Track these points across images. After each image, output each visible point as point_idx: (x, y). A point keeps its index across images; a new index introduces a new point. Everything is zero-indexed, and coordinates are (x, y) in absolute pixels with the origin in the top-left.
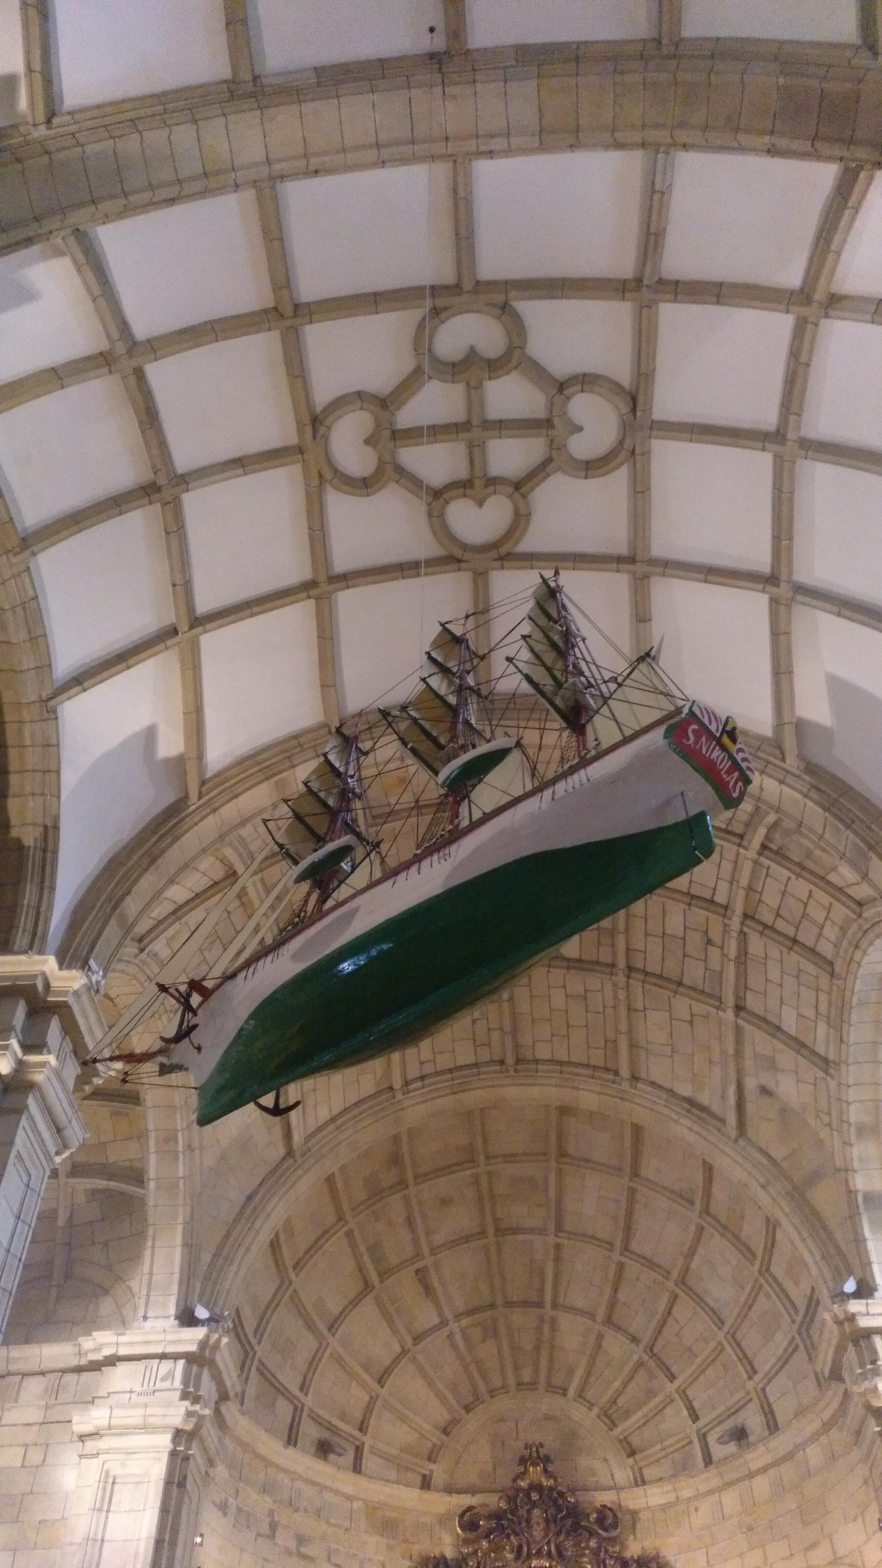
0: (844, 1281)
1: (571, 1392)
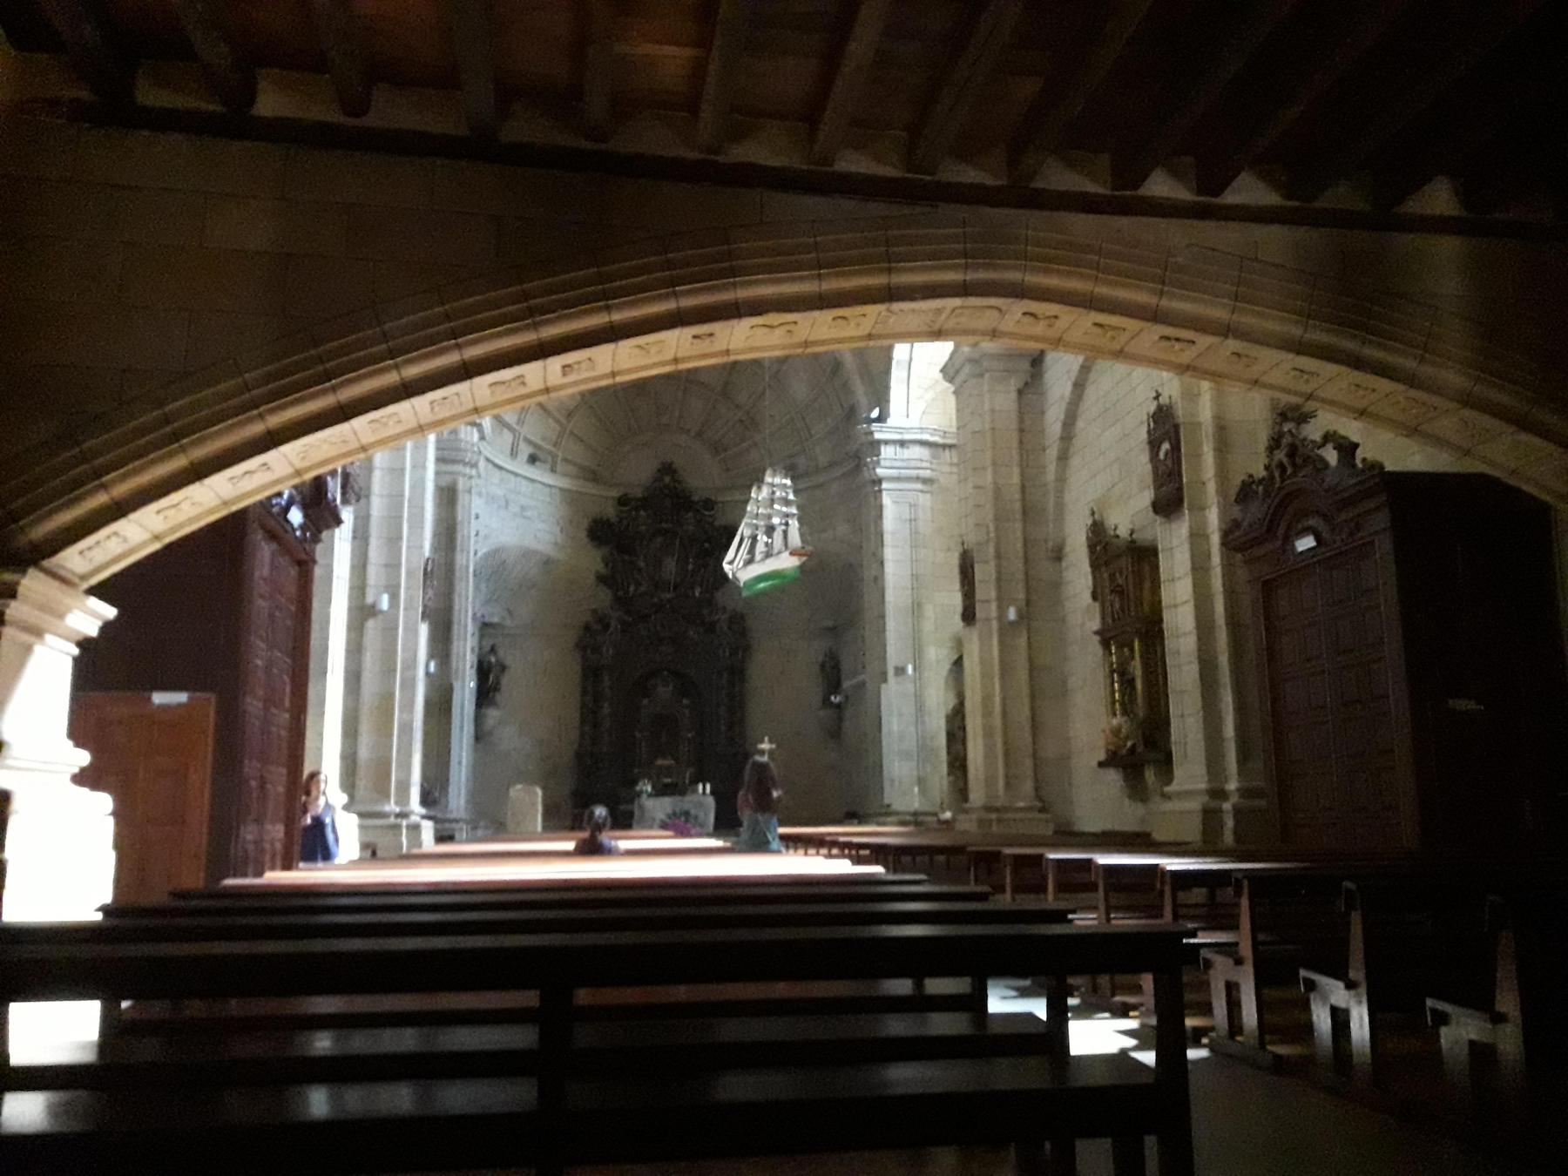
0: (871, 410)
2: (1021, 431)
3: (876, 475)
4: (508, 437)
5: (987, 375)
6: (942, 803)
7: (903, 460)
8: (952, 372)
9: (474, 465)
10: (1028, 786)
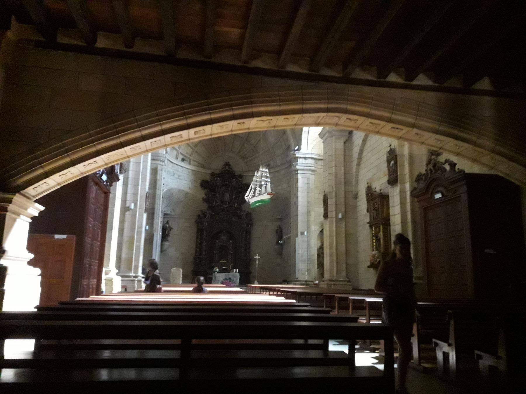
1: (236, 153)
2: (345, 155)
3: (296, 168)
4: (175, 152)
5: (334, 137)
6: (315, 278)
7: (305, 164)
8: (322, 136)
9: (164, 161)
10: (344, 273)
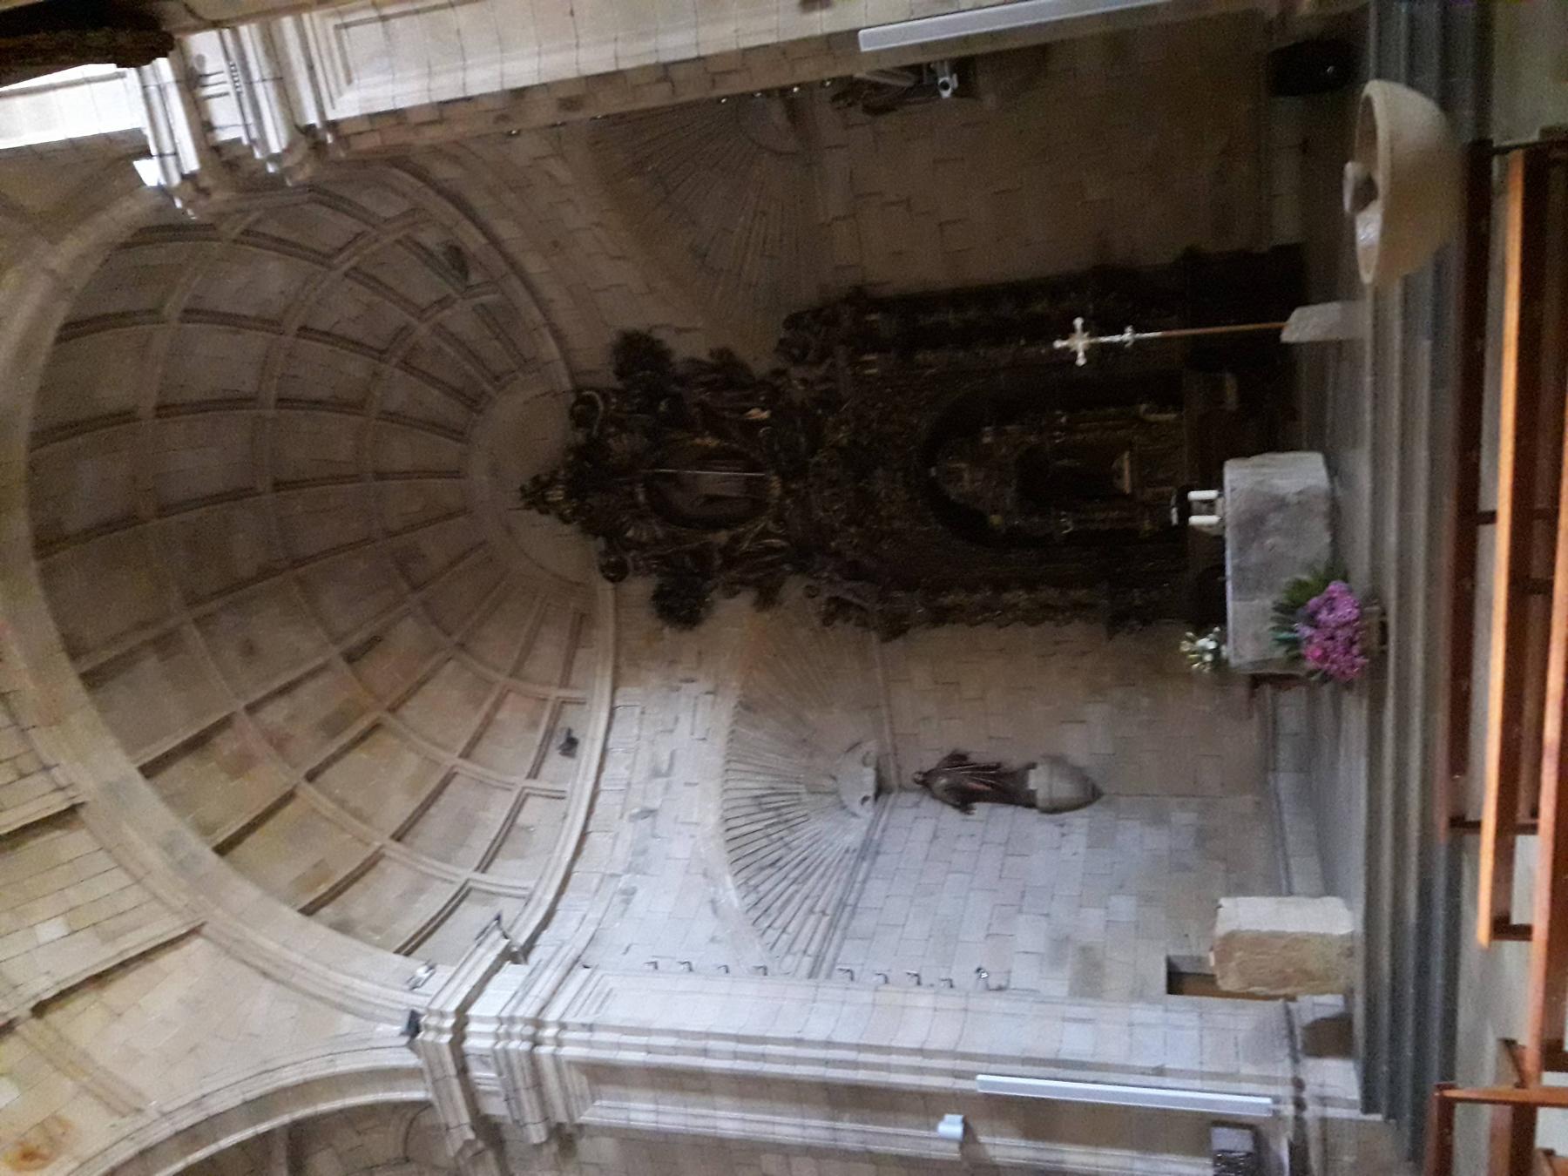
3: (288, 150)
